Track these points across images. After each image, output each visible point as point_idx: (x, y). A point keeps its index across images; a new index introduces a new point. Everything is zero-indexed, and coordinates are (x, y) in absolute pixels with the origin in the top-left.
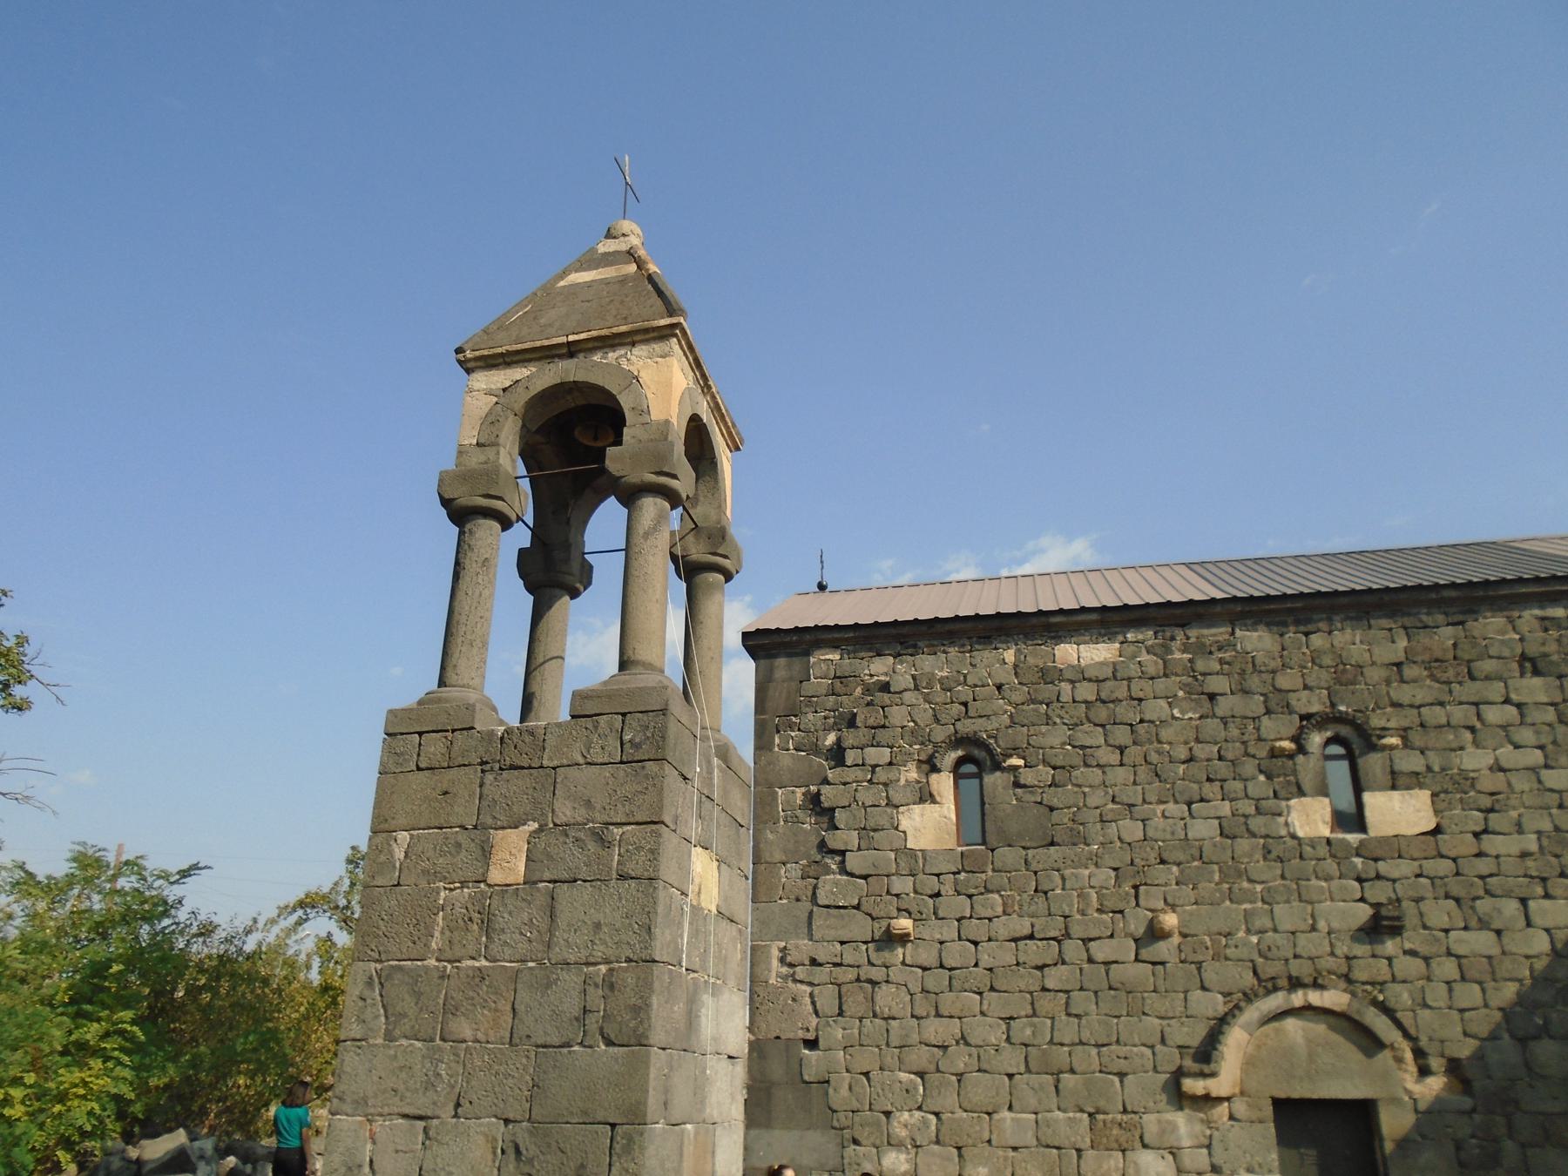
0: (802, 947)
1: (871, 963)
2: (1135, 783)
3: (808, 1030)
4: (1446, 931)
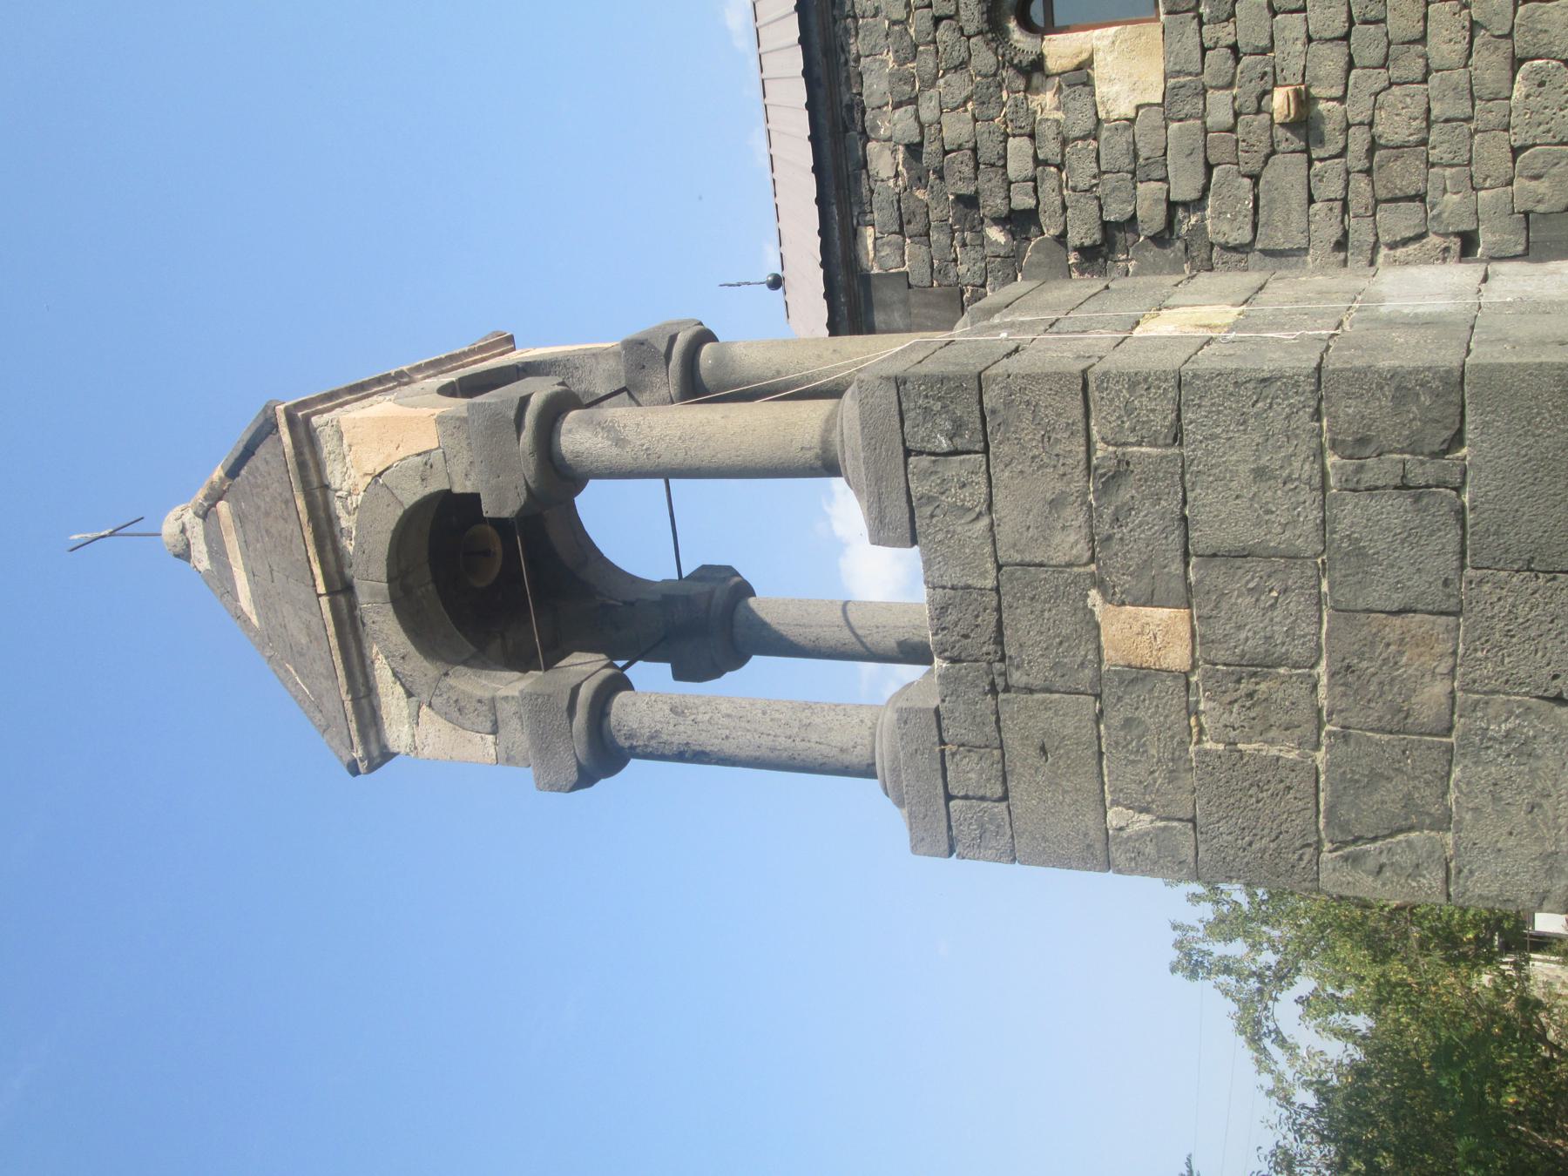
1: (1342, 153)
3: (1447, 249)
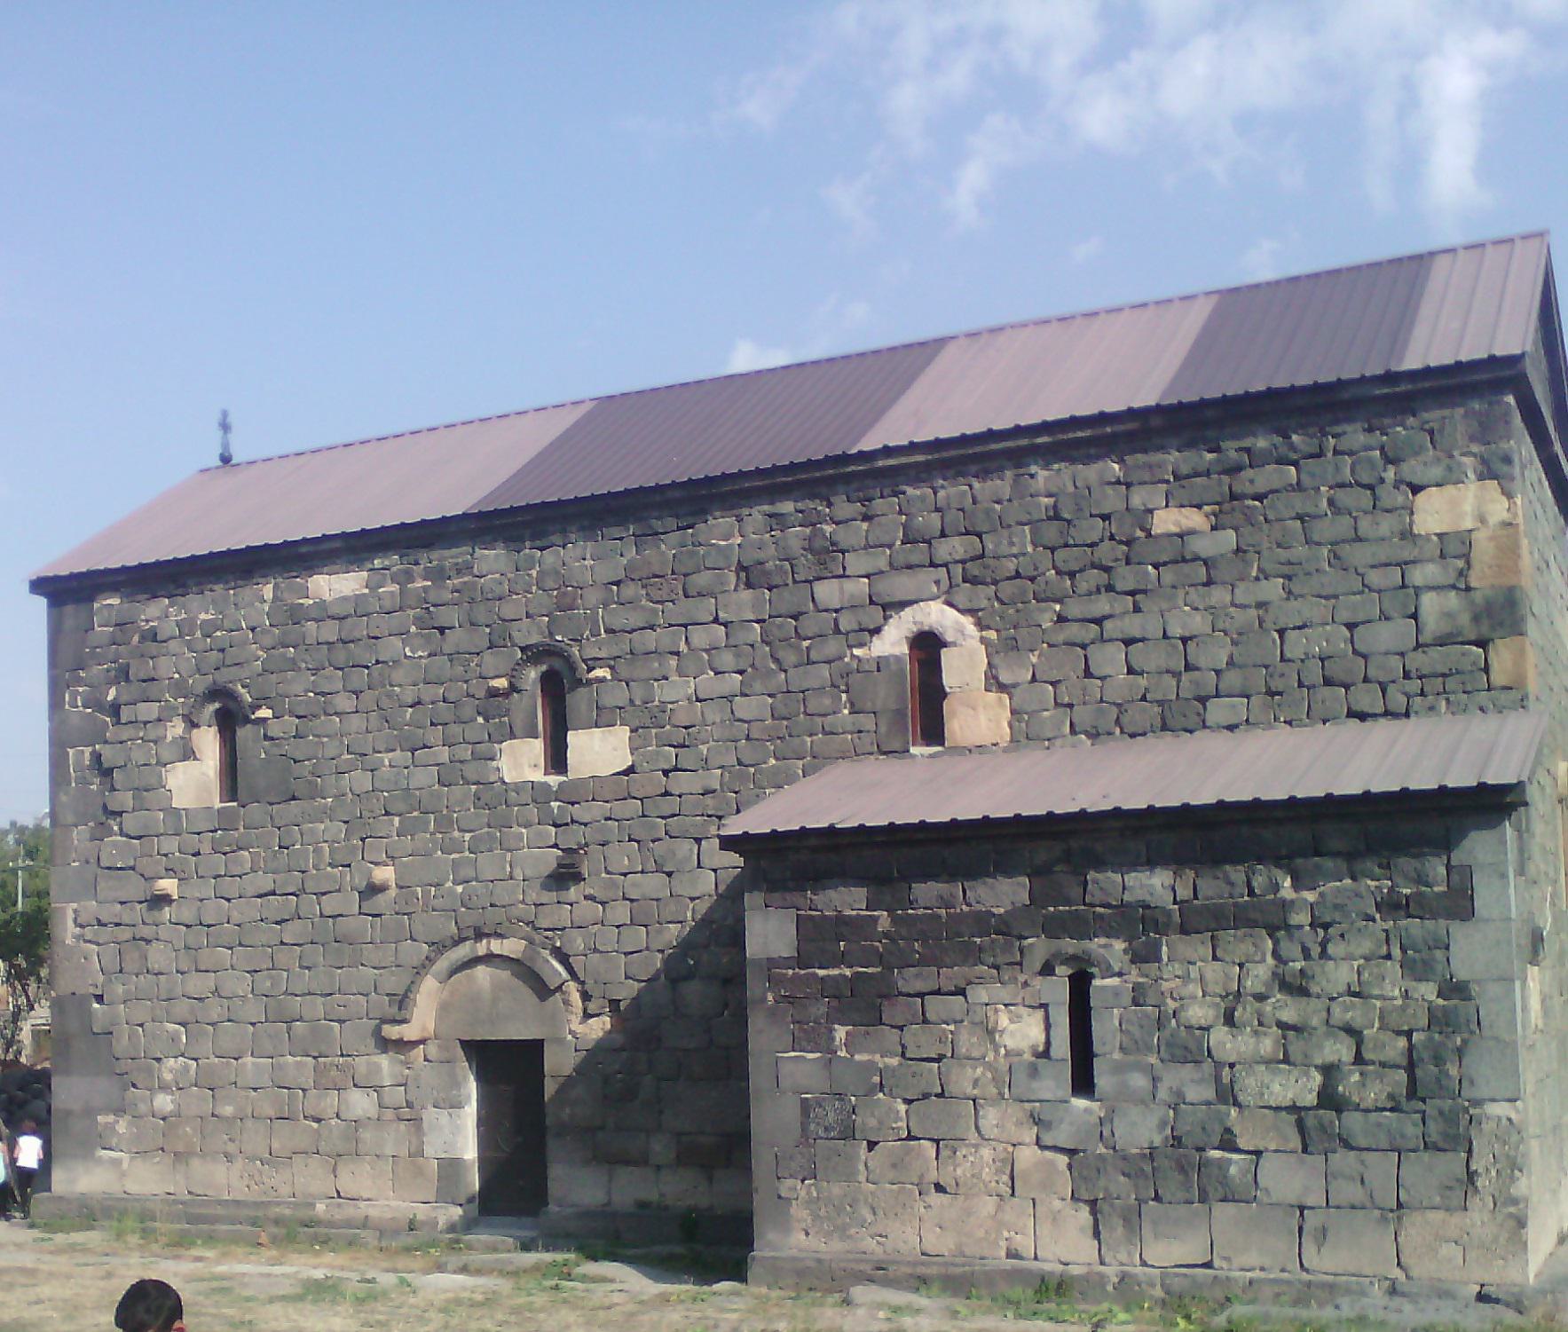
1: (144, 923)
2: (368, 731)
4: (625, 875)
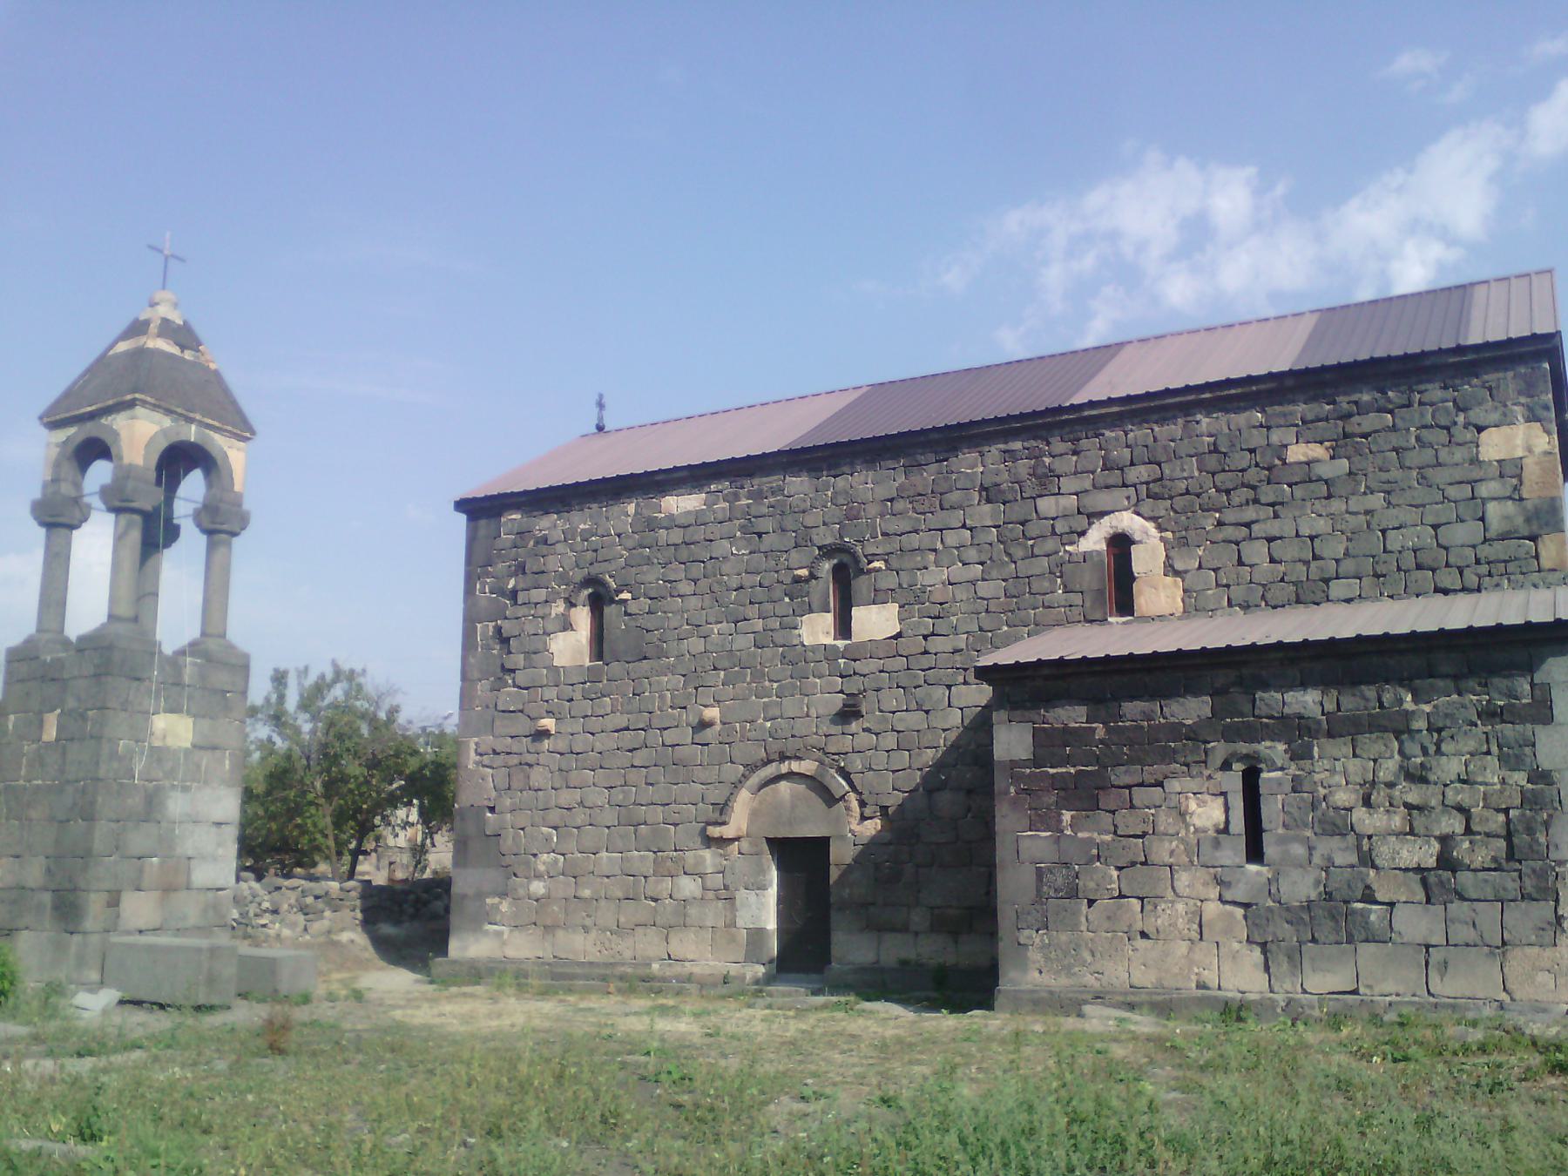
0: (489, 741)
1: (528, 752)
4: (894, 713)
